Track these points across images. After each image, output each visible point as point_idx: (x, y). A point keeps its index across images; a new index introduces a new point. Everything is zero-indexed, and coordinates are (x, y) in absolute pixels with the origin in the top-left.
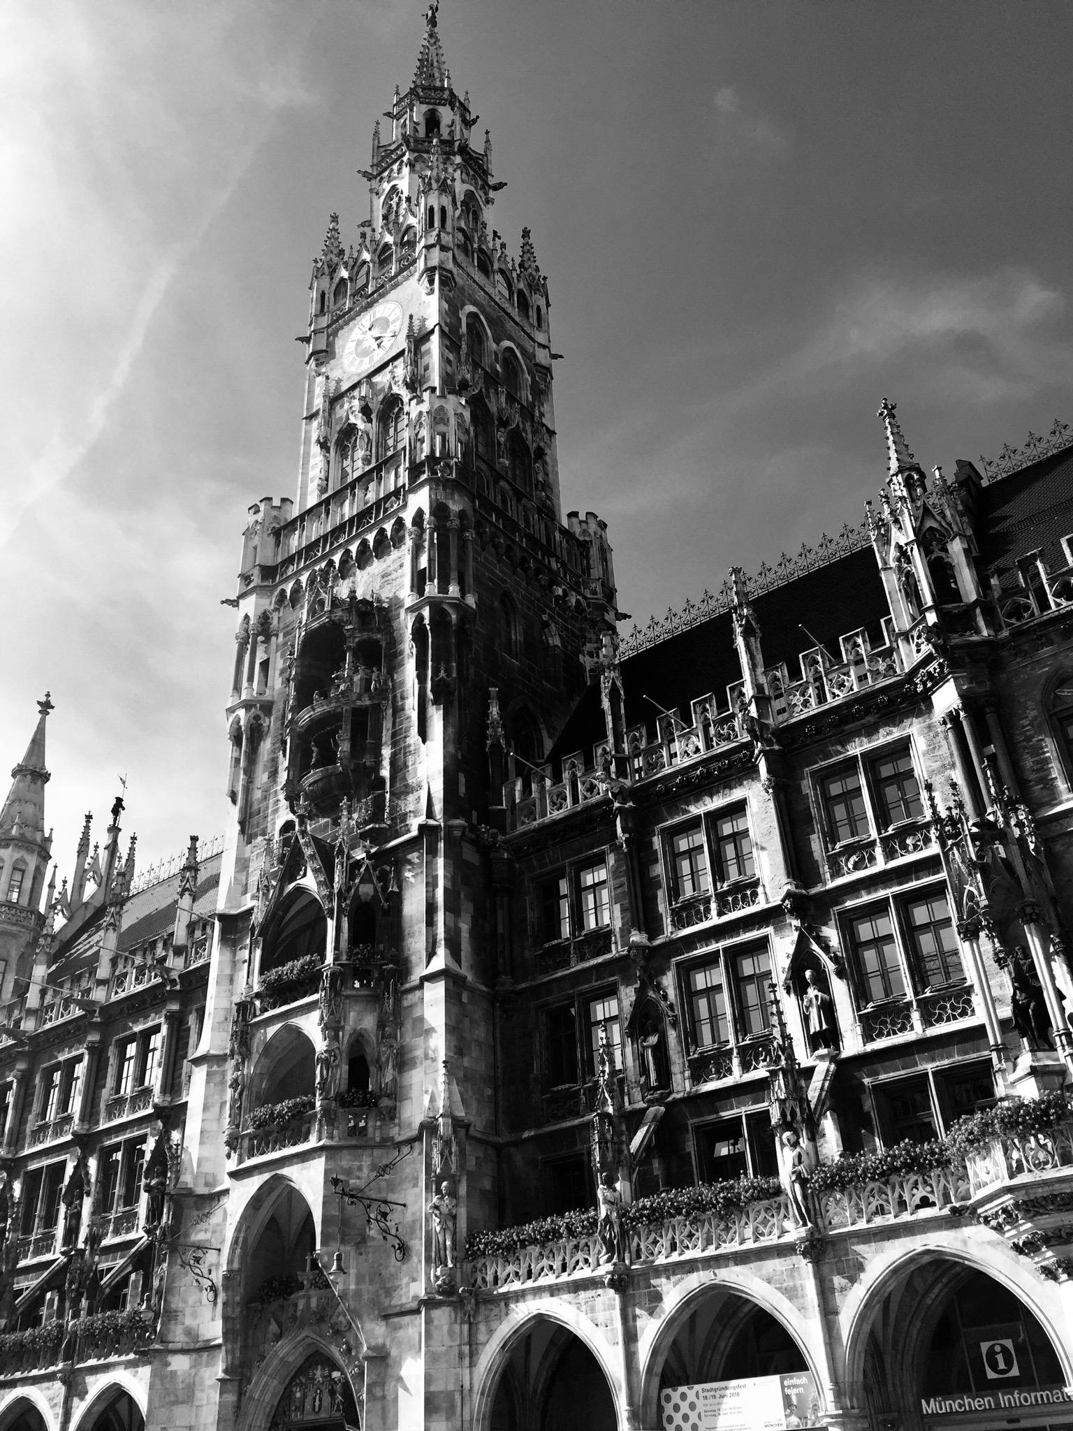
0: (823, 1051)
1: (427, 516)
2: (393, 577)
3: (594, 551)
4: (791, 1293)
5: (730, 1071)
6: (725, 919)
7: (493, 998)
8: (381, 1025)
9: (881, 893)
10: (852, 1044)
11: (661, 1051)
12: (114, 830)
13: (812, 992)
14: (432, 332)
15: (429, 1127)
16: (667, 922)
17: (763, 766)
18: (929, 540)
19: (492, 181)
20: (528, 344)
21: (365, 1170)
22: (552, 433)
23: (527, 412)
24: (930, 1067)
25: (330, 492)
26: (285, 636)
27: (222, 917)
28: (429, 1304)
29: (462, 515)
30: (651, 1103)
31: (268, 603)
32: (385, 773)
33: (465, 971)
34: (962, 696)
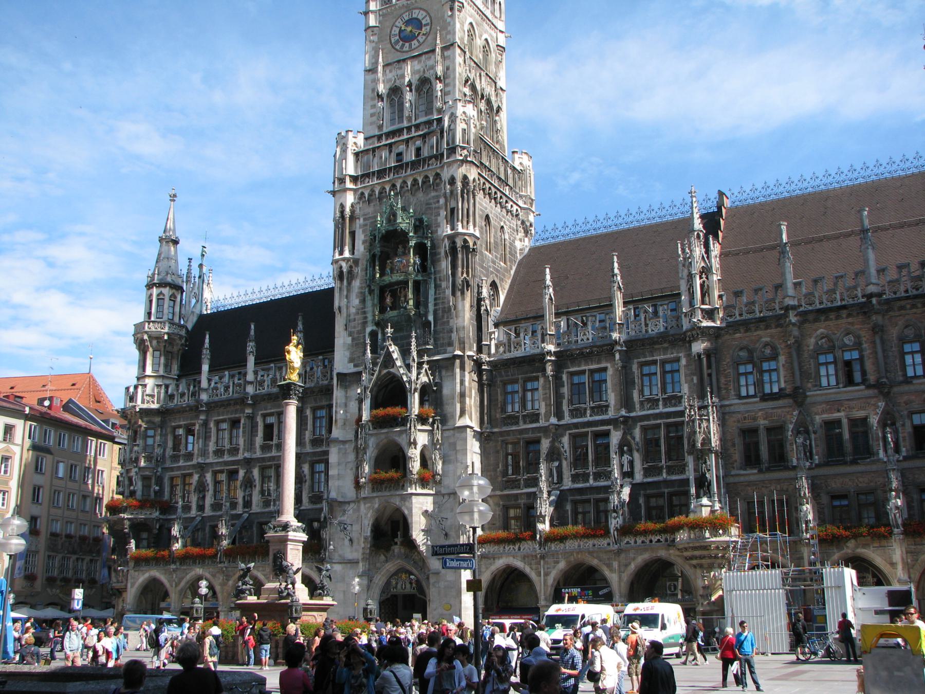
0: (627, 479)
2: (434, 206)
5: (588, 481)
6: (591, 419)
9: (659, 421)
10: (639, 477)
11: (559, 469)
12: (201, 266)
16: (566, 414)
17: (617, 356)
24: (666, 491)
25: (385, 130)
26: (364, 220)
27: (339, 374)
29: (474, 180)
30: (554, 489)
32: (431, 318)
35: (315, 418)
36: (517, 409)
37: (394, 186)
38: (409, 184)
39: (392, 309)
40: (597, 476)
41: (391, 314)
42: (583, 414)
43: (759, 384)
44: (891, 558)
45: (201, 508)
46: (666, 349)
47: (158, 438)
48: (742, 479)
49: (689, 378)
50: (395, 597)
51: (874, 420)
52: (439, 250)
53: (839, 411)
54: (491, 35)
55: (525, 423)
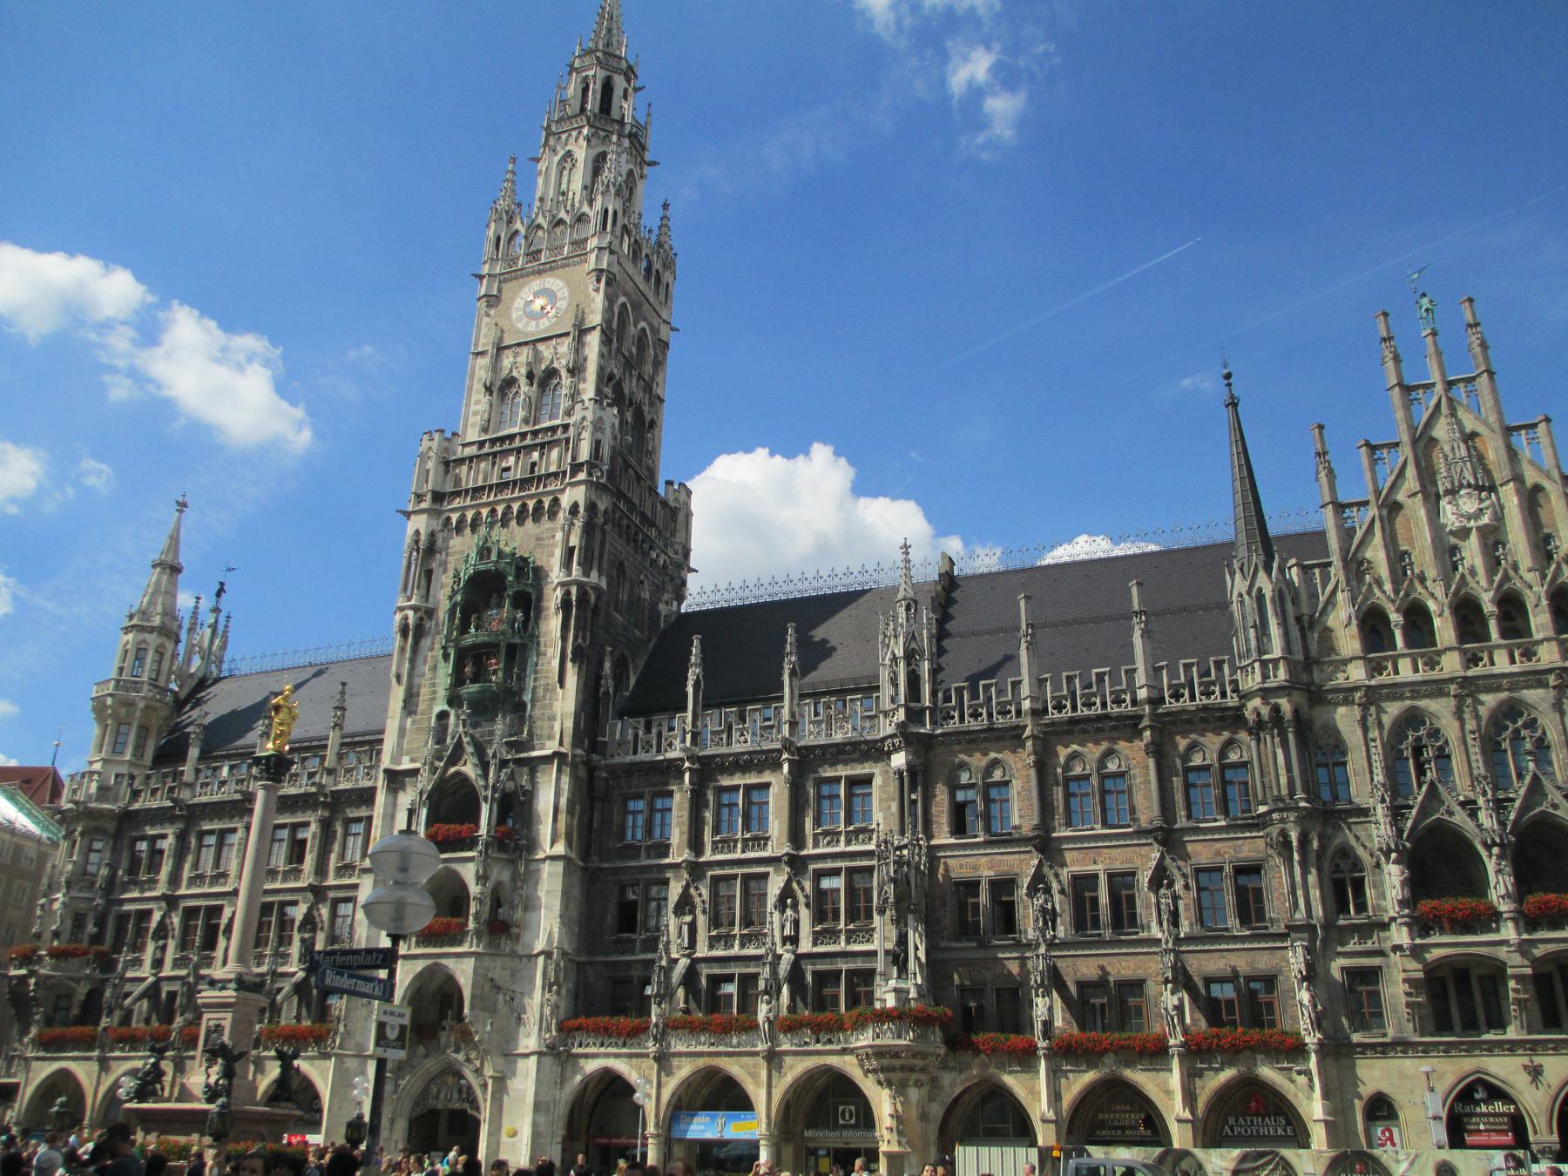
1: (582, 509)
3: (681, 517)
4: (755, 1076)
6: (744, 856)
7: (585, 869)
8: (513, 879)
10: (805, 946)
11: (693, 927)
13: (789, 912)
14: (594, 328)
15: (547, 954)
18: (910, 656)
19: (648, 157)
20: (656, 321)
21: (498, 970)
22: (661, 400)
23: (648, 389)
24: (844, 967)
27: (386, 771)
28: (540, 1054)
31: (437, 525)
32: (527, 697)
33: (573, 855)
35: (346, 834)
36: (639, 835)
37: (493, 511)
38: (516, 507)
39: (473, 682)
40: (745, 940)
41: (471, 688)
42: (733, 850)
44: (1166, 1082)
45: (158, 963)
47: (108, 854)
48: (954, 955)
50: (434, 1114)
52: (545, 604)
54: (650, 324)
55: (649, 856)
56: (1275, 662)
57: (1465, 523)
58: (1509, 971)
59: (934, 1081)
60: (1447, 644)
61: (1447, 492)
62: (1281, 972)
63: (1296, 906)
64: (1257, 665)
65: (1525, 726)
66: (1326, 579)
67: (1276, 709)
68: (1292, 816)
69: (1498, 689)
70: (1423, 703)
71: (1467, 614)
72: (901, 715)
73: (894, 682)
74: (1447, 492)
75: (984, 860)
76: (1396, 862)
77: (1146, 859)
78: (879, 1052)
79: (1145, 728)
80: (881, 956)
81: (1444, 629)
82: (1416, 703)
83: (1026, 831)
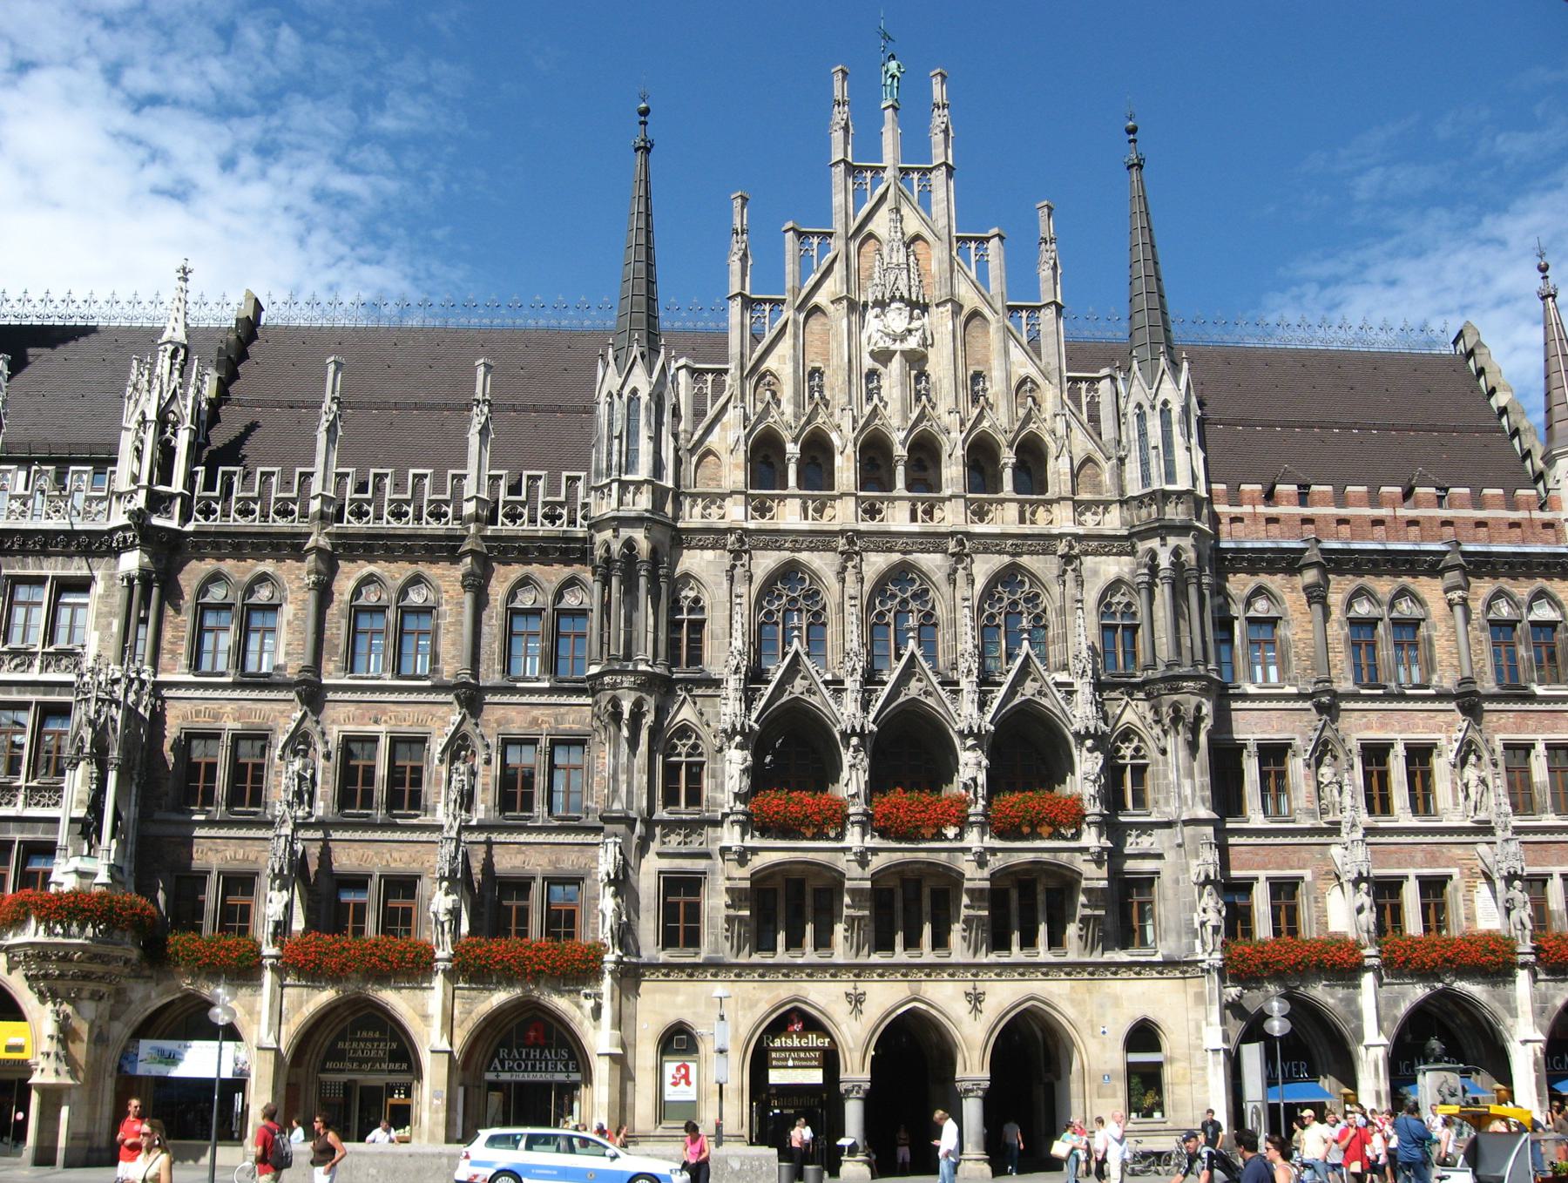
18: (163, 420)
24: (18, 837)
34: (141, 569)
43: (241, 650)
46: (70, 556)
49: (103, 621)
51: (437, 745)
53: (376, 722)
56: (638, 485)
57: (888, 343)
58: (848, 884)
59: (120, 994)
60: (844, 489)
61: (876, 303)
62: (589, 873)
63: (615, 791)
64: (615, 486)
65: (915, 596)
66: (719, 388)
67: (629, 544)
68: (628, 681)
69: (890, 550)
70: (804, 556)
71: (874, 453)
72: (140, 501)
73: (139, 453)
74: (876, 303)
75: (229, 707)
76: (740, 747)
77: (443, 721)
78: (41, 954)
79: (465, 554)
80: (64, 826)
81: (845, 469)
82: (797, 555)
83: (292, 673)
